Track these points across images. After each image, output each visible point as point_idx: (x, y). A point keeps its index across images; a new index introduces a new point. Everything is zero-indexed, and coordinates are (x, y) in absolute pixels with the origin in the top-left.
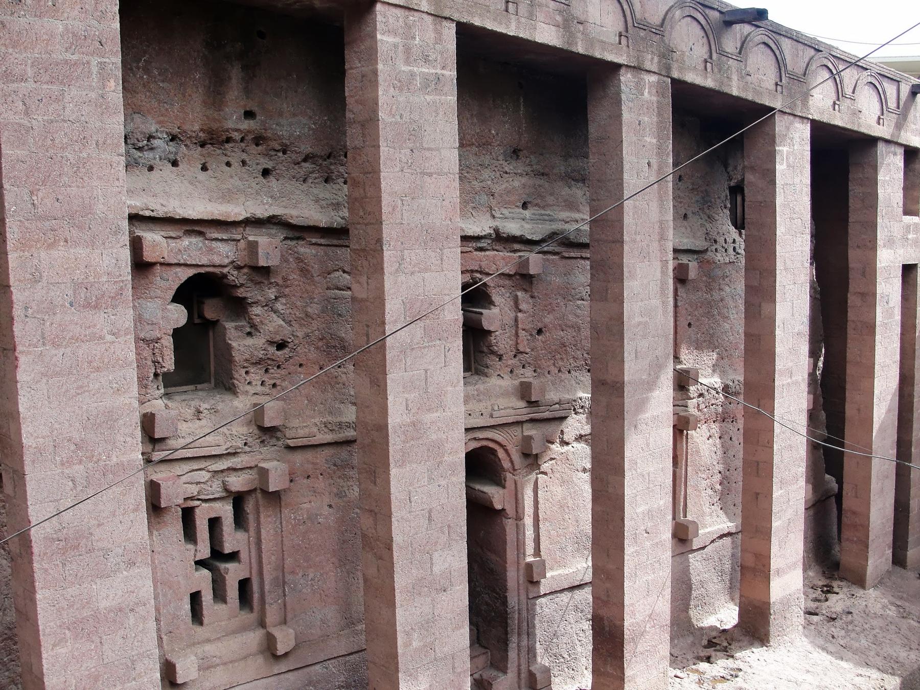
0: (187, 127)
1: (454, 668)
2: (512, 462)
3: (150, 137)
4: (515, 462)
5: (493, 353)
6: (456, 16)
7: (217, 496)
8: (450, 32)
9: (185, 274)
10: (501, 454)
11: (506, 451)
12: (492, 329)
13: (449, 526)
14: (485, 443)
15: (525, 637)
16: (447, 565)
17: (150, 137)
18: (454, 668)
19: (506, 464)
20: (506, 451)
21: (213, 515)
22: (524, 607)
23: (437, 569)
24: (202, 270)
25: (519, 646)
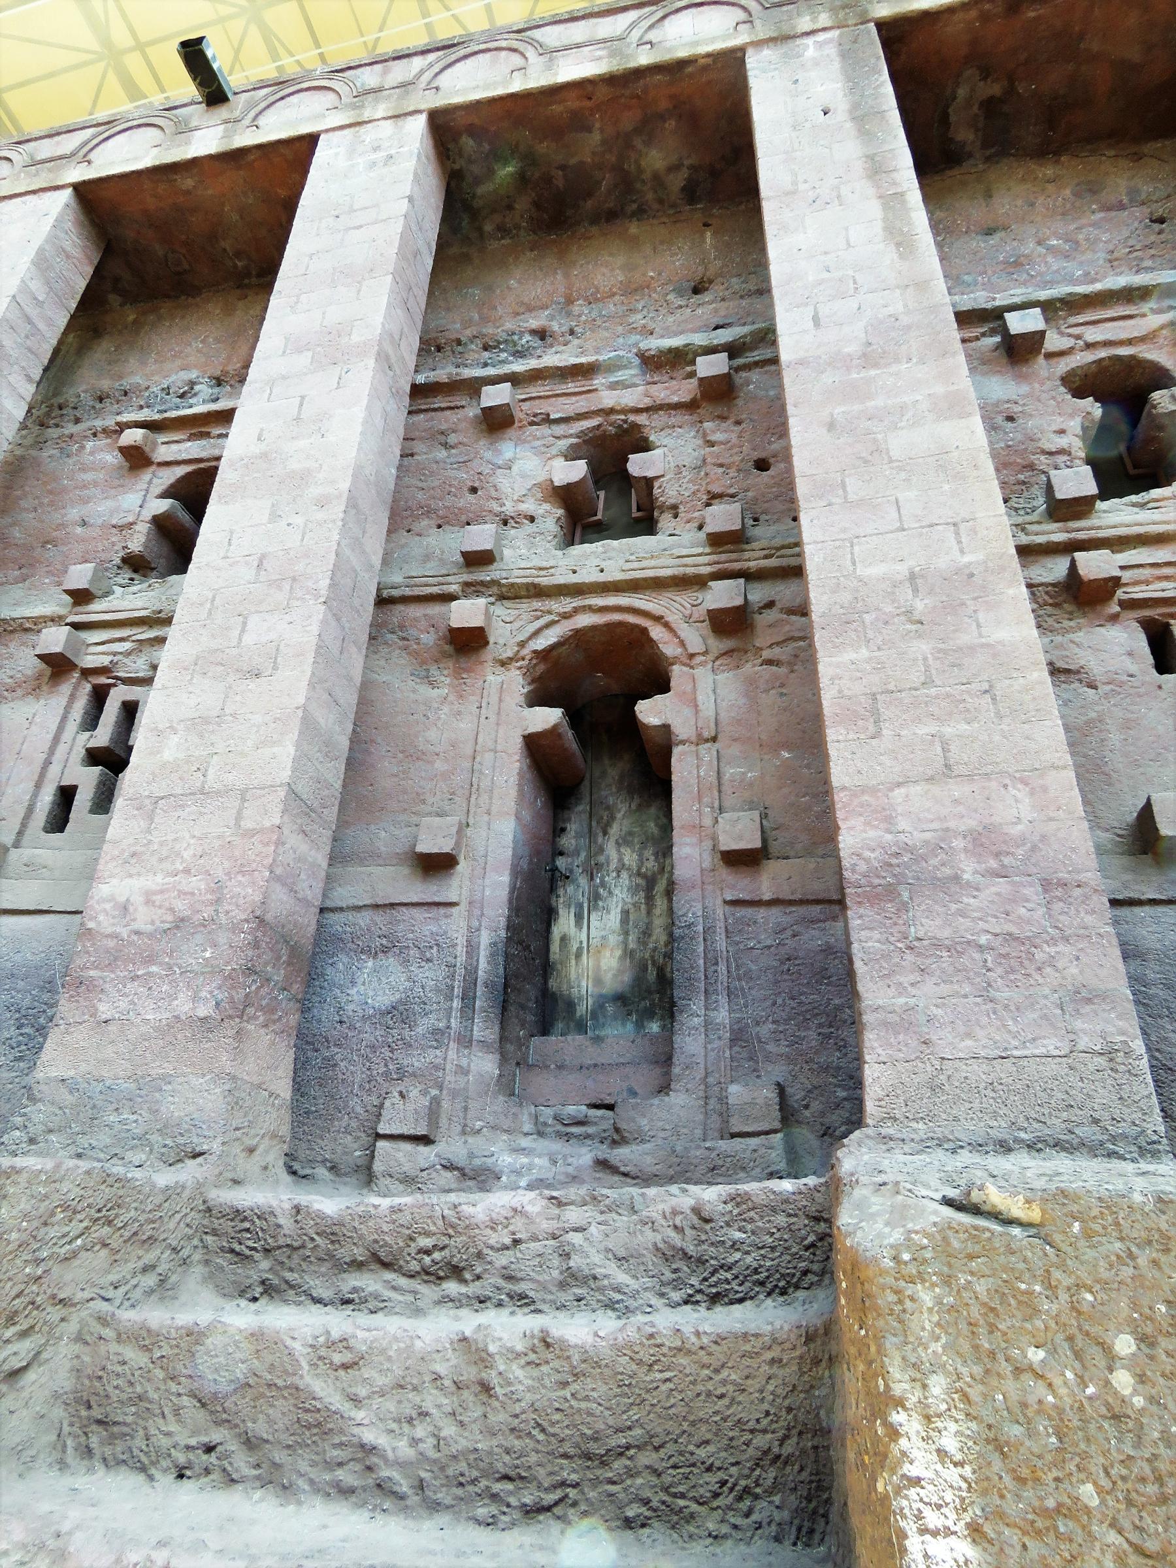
0: (230, 368)
1: (239, 817)
2: (682, 643)
3: (192, 384)
4: (687, 642)
5: (663, 509)
6: (422, 107)
7: (141, 674)
8: (418, 125)
9: (181, 471)
10: (656, 632)
11: (667, 625)
12: (650, 474)
13: (294, 579)
14: (616, 617)
15: (723, 1000)
16: (273, 636)
17: (192, 384)
18: (239, 817)
19: (669, 649)
20: (667, 625)
21: (128, 698)
22: (720, 925)
23: (248, 639)
24: (202, 465)
25: (707, 1024)
